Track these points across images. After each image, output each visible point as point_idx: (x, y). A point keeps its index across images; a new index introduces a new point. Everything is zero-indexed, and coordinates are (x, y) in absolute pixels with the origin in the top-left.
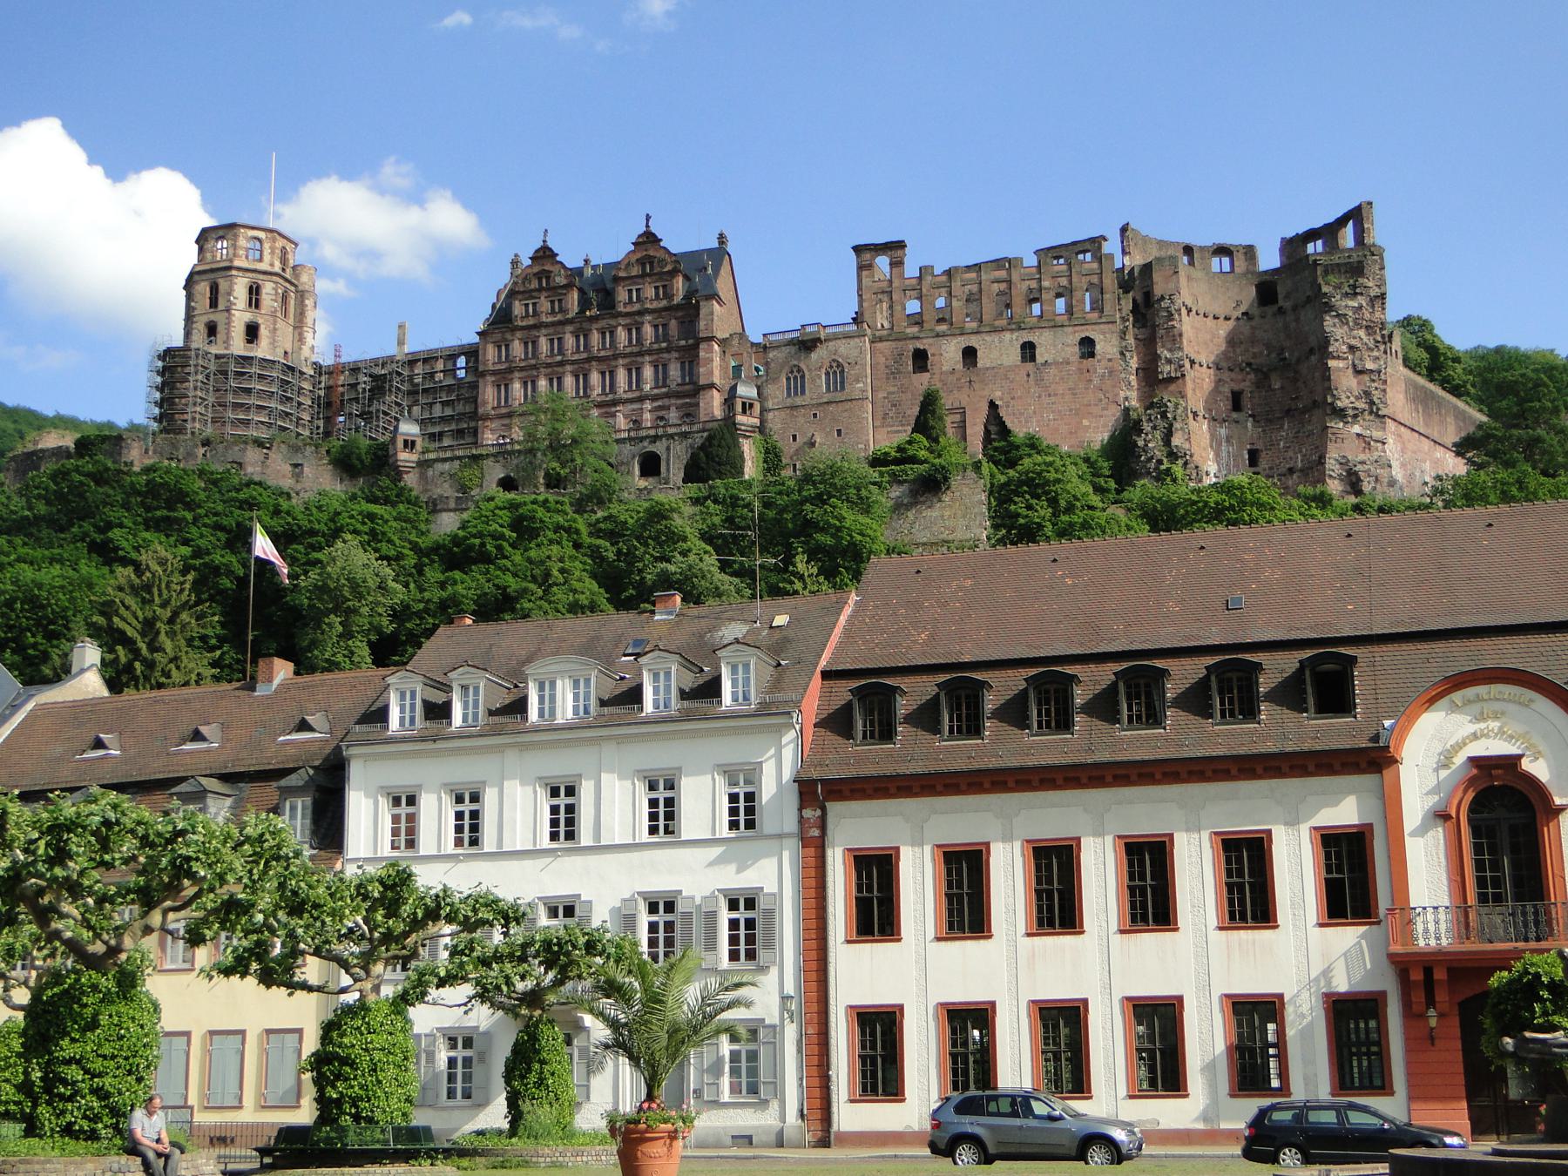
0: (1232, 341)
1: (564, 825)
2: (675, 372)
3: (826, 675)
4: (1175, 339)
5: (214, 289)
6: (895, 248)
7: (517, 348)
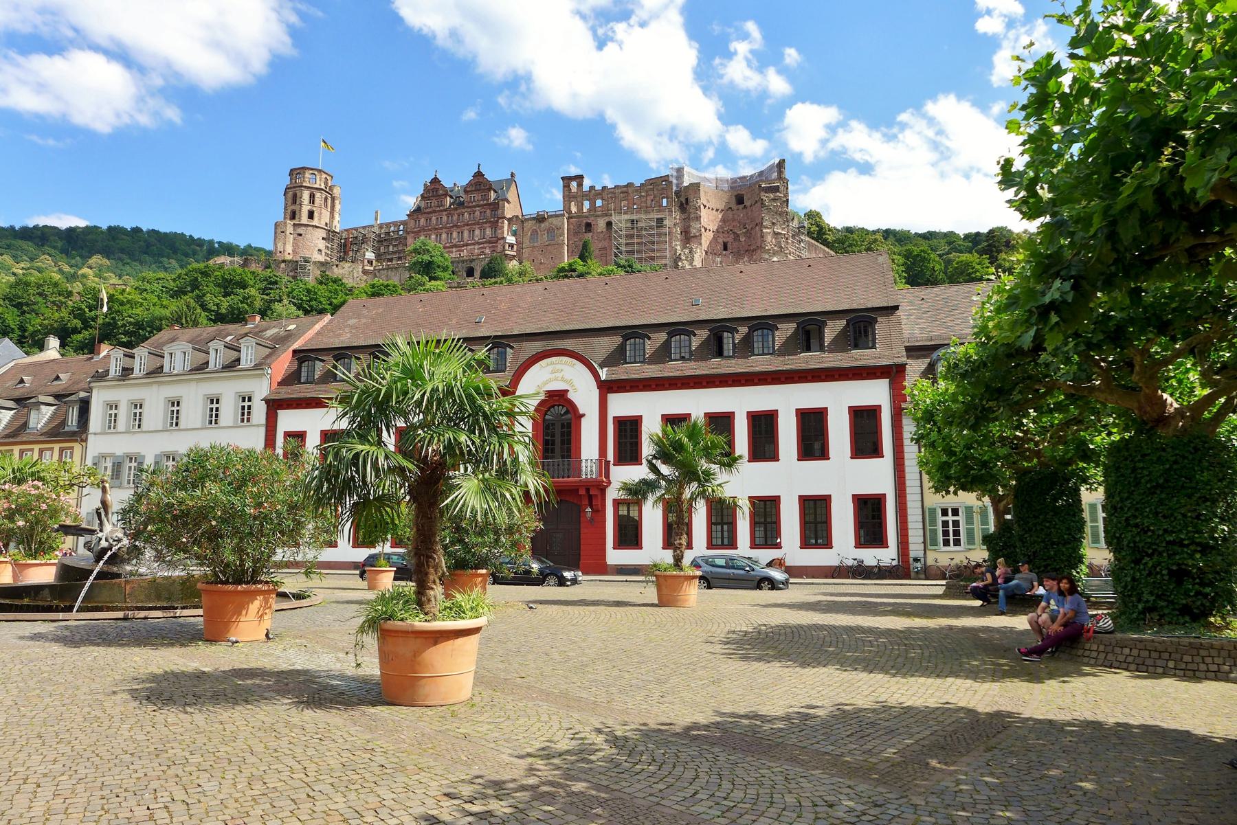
0: (723, 220)
1: (175, 419)
2: (488, 232)
3: (295, 352)
4: (698, 218)
5: (295, 196)
6: (580, 178)
7: (422, 221)
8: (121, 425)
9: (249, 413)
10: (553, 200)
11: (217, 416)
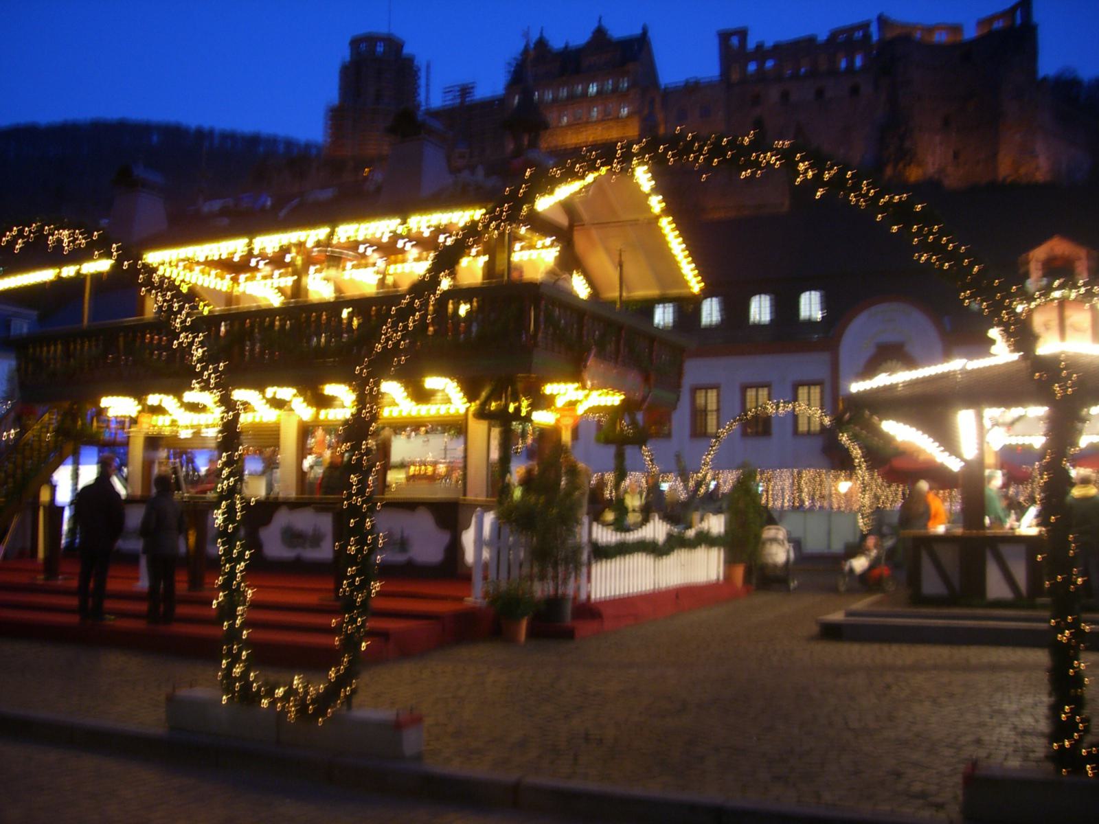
6: (742, 34)
10: (708, 67)
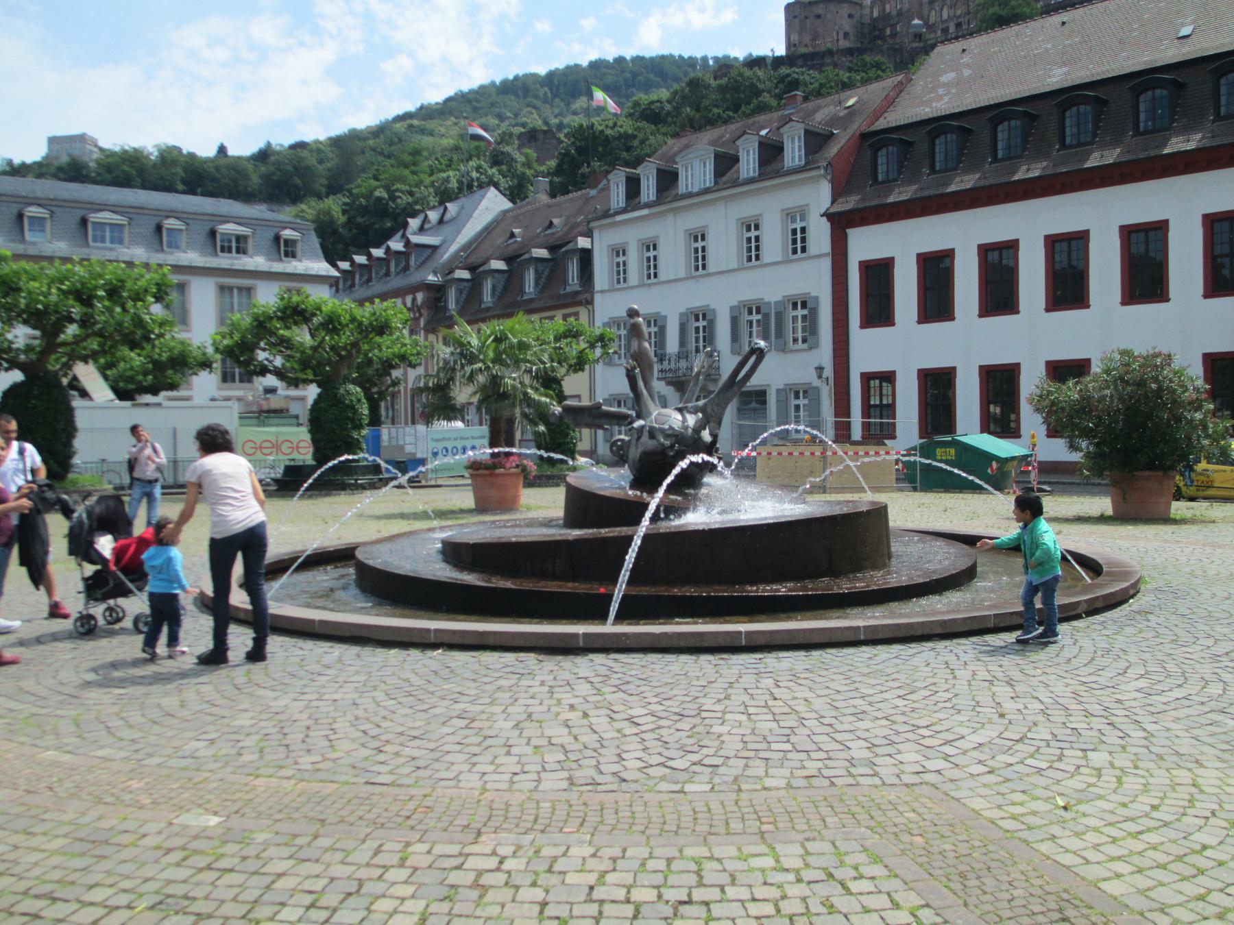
1: (699, 260)
8: (634, 276)
9: (803, 240)
11: (757, 248)
